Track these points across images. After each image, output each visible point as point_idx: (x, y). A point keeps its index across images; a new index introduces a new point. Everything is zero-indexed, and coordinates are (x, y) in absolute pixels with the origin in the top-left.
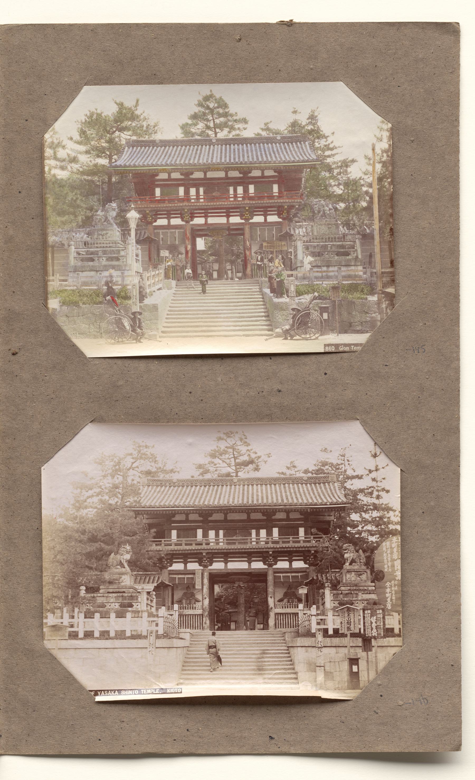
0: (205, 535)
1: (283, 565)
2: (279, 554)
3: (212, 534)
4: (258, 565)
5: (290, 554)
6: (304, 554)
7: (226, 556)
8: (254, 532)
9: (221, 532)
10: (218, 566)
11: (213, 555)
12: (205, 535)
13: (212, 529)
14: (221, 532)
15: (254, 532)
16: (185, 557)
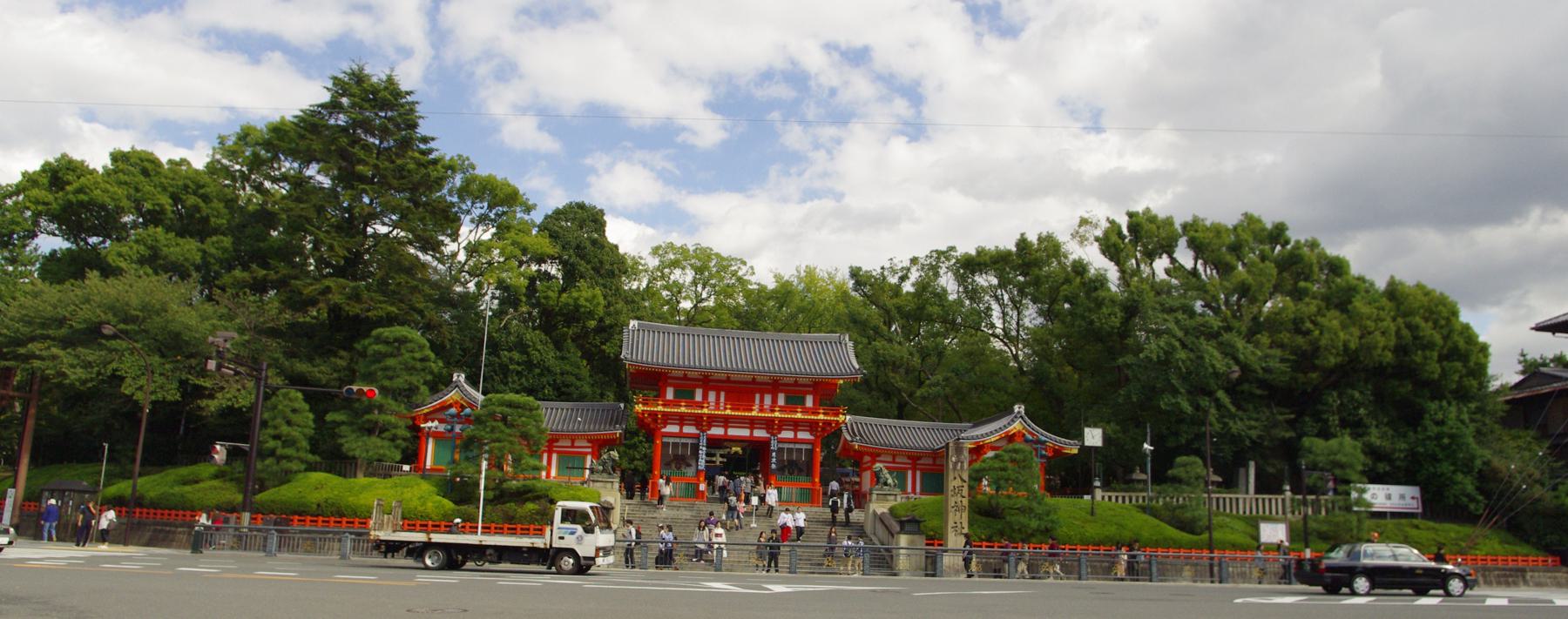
0: (705, 397)
1: (787, 434)
2: (783, 424)
3: (712, 396)
4: (760, 433)
5: (796, 425)
6: (812, 426)
7: (726, 422)
8: (757, 397)
9: (723, 394)
10: (717, 431)
11: (712, 420)
12: (705, 397)
13: (713, 388)
14: (723, 394)
15: (757, 397)
16: (682, 419)
